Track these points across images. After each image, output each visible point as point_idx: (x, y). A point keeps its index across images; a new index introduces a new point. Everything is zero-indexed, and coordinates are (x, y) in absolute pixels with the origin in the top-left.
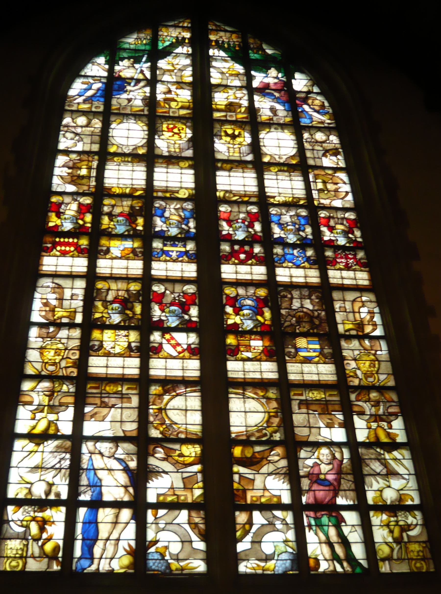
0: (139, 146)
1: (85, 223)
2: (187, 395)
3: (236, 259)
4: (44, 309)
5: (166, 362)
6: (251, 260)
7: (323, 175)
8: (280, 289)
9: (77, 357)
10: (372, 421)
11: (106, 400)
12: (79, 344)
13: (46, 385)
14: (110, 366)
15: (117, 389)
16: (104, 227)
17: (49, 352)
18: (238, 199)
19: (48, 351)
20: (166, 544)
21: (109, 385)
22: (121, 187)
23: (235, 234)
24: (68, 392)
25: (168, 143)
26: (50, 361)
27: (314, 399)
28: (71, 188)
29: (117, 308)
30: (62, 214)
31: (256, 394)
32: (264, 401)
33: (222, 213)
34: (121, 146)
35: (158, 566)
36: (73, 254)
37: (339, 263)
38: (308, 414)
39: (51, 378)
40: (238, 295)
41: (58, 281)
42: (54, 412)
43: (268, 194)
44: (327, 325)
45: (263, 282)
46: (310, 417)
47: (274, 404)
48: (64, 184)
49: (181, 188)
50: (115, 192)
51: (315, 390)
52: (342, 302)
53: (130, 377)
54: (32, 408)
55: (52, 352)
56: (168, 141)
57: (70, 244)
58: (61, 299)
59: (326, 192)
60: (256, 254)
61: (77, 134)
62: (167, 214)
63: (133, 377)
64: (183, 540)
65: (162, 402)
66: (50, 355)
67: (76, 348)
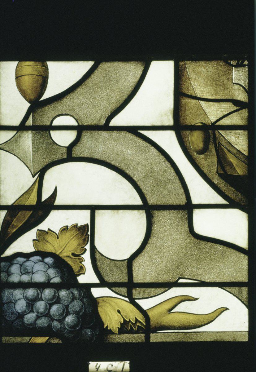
20: (83, 218)
35: (47, 314)
64: (152, 200)
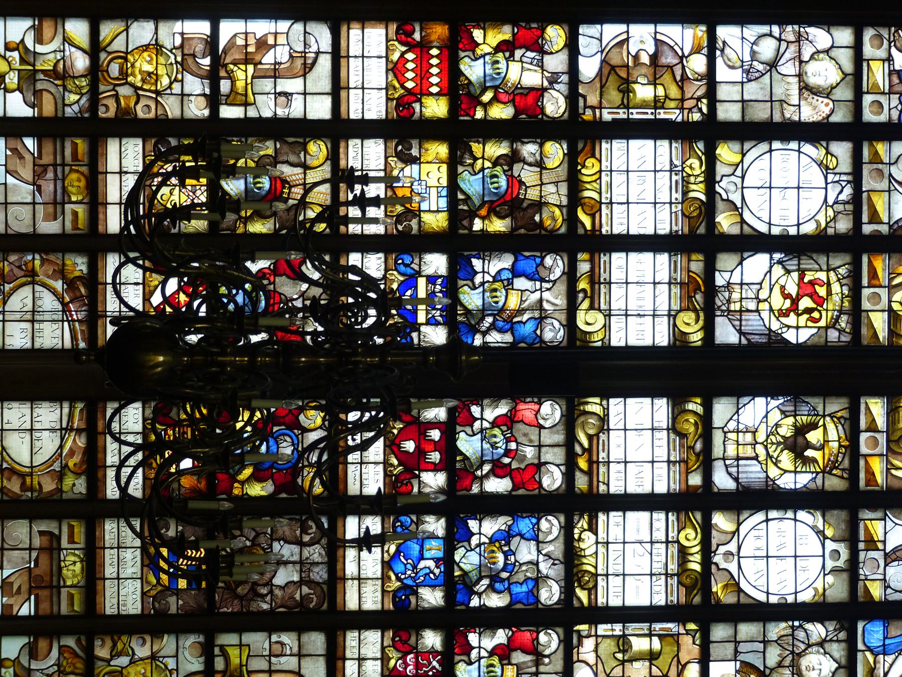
0: (741, 215)
1: (485, 106)
2: (66, 324)
3: (400, 430)
4: (251, 41)
5: (137, 284)
6: (399, 465)
7: (677, 655)
8: (324, 520)
9: (141, 114)
10: (18, 672)
11: (50, 175)
12: (170, 116)
13: (81, 62)
14: (124, 178)
15: (75, 194)
16: (476, 148)
17: (150, 62)
18: (581, 445)
19: (152, 59)
21: (83, 179)
22: (600, 178)
23: (474, 435)
24: (64, 105)
25: (761, 284)
26: (129, 65)
27: (63, 564)
28: (589, 68)
29: (258, 185)
30: (507, 54)
31: (72, 453)
32: (57, 466)
33: (536, 407)
34: (739, 172)
36: (395, 88)
37: (404, 658)
38: (30, 549)
39: (95, 71)
40: (305, 430)
41: (325, 64)
42: (21, 83)
43: (602, 517)
44: (235, 610)
45: (341, 487)
46: (24, 552)
47: (49, 486)
48: (602, 52)
49: (608, 315)
50: (584, 166)
51: (82, 568)
52: (295, 650)
53: (101, 216)
54: (29, 43)
55: (150, 68)
56: (766, 285)
57: (421, 79)
58: (275, 73)
59: (620, 656)
60: (419, 477)
61: (773, 65)
62: (521, 283)
63: (101, 222)
65: (48, 277)
66: (144, 63)
67: (159, 113)
